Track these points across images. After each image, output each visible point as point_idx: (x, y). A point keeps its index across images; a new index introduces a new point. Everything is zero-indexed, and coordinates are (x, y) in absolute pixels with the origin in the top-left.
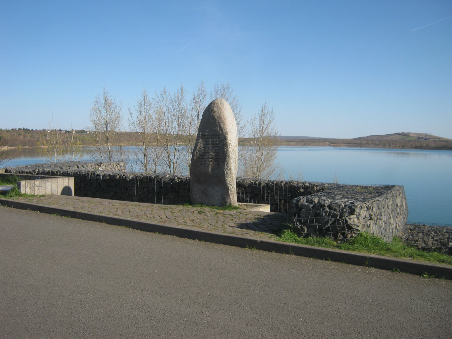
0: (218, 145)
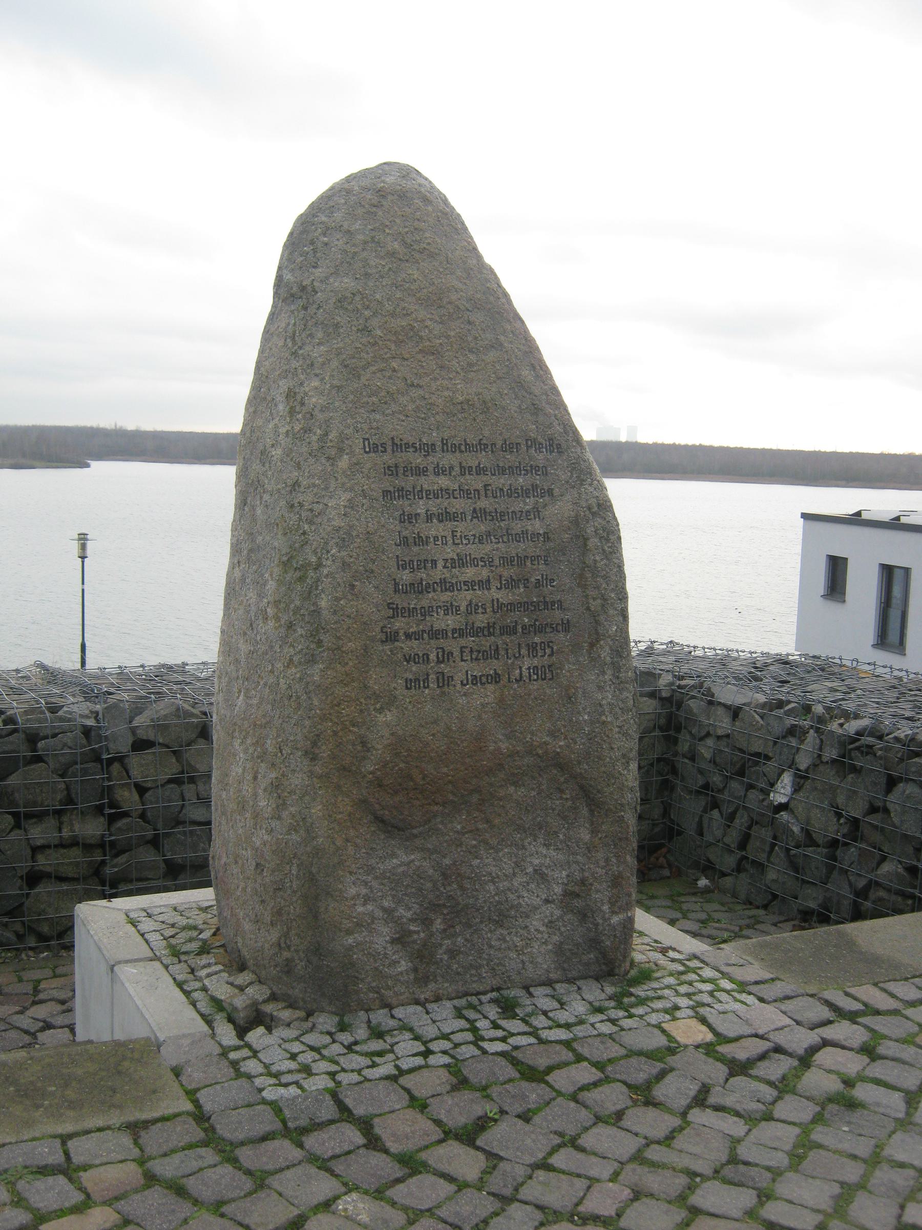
0: (537, 526)
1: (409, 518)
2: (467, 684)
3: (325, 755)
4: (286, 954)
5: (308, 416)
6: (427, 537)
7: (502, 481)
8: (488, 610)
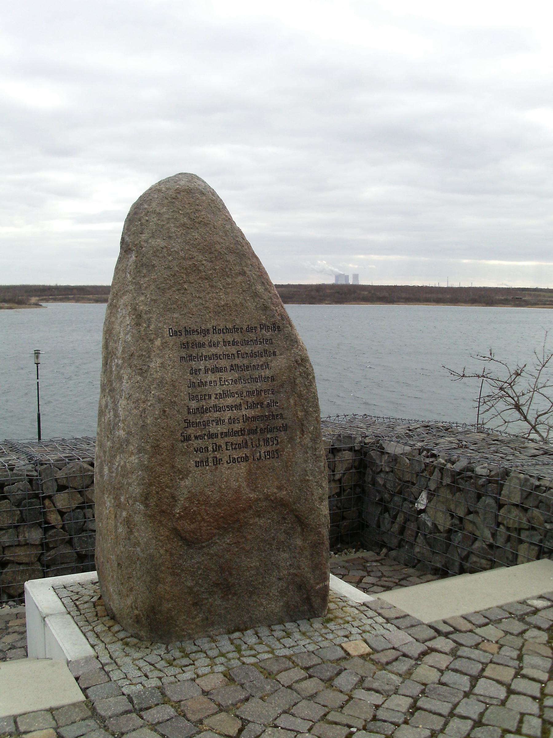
0: (267, 373)
1: (195, 372)
2: (230, 462)
3: (152, 504)
4: (136, 612)
5: (139, 317)
6: (206, 382)
7: (248, 349)
8: (240, 421)
